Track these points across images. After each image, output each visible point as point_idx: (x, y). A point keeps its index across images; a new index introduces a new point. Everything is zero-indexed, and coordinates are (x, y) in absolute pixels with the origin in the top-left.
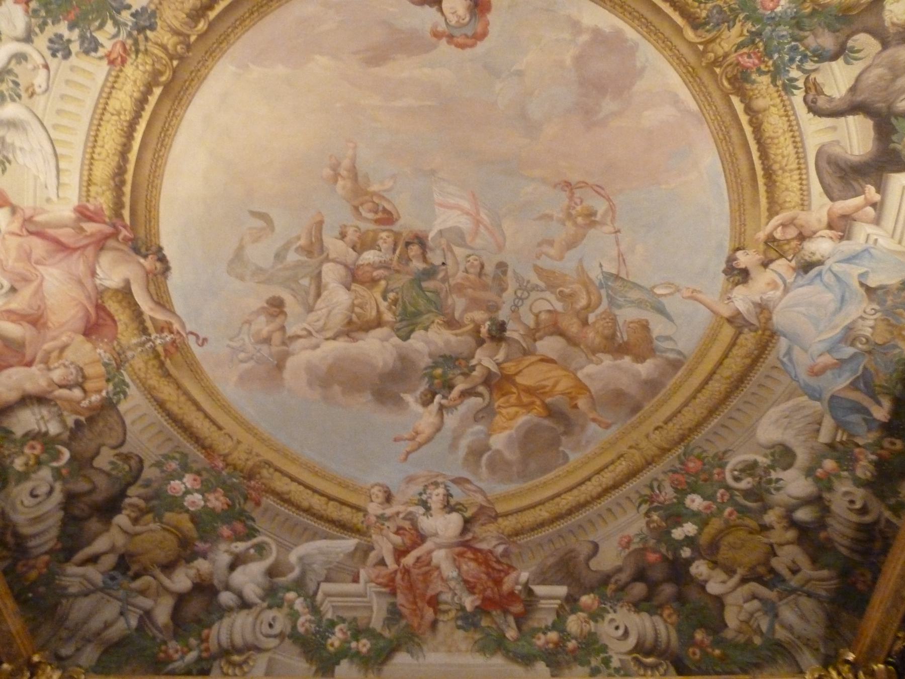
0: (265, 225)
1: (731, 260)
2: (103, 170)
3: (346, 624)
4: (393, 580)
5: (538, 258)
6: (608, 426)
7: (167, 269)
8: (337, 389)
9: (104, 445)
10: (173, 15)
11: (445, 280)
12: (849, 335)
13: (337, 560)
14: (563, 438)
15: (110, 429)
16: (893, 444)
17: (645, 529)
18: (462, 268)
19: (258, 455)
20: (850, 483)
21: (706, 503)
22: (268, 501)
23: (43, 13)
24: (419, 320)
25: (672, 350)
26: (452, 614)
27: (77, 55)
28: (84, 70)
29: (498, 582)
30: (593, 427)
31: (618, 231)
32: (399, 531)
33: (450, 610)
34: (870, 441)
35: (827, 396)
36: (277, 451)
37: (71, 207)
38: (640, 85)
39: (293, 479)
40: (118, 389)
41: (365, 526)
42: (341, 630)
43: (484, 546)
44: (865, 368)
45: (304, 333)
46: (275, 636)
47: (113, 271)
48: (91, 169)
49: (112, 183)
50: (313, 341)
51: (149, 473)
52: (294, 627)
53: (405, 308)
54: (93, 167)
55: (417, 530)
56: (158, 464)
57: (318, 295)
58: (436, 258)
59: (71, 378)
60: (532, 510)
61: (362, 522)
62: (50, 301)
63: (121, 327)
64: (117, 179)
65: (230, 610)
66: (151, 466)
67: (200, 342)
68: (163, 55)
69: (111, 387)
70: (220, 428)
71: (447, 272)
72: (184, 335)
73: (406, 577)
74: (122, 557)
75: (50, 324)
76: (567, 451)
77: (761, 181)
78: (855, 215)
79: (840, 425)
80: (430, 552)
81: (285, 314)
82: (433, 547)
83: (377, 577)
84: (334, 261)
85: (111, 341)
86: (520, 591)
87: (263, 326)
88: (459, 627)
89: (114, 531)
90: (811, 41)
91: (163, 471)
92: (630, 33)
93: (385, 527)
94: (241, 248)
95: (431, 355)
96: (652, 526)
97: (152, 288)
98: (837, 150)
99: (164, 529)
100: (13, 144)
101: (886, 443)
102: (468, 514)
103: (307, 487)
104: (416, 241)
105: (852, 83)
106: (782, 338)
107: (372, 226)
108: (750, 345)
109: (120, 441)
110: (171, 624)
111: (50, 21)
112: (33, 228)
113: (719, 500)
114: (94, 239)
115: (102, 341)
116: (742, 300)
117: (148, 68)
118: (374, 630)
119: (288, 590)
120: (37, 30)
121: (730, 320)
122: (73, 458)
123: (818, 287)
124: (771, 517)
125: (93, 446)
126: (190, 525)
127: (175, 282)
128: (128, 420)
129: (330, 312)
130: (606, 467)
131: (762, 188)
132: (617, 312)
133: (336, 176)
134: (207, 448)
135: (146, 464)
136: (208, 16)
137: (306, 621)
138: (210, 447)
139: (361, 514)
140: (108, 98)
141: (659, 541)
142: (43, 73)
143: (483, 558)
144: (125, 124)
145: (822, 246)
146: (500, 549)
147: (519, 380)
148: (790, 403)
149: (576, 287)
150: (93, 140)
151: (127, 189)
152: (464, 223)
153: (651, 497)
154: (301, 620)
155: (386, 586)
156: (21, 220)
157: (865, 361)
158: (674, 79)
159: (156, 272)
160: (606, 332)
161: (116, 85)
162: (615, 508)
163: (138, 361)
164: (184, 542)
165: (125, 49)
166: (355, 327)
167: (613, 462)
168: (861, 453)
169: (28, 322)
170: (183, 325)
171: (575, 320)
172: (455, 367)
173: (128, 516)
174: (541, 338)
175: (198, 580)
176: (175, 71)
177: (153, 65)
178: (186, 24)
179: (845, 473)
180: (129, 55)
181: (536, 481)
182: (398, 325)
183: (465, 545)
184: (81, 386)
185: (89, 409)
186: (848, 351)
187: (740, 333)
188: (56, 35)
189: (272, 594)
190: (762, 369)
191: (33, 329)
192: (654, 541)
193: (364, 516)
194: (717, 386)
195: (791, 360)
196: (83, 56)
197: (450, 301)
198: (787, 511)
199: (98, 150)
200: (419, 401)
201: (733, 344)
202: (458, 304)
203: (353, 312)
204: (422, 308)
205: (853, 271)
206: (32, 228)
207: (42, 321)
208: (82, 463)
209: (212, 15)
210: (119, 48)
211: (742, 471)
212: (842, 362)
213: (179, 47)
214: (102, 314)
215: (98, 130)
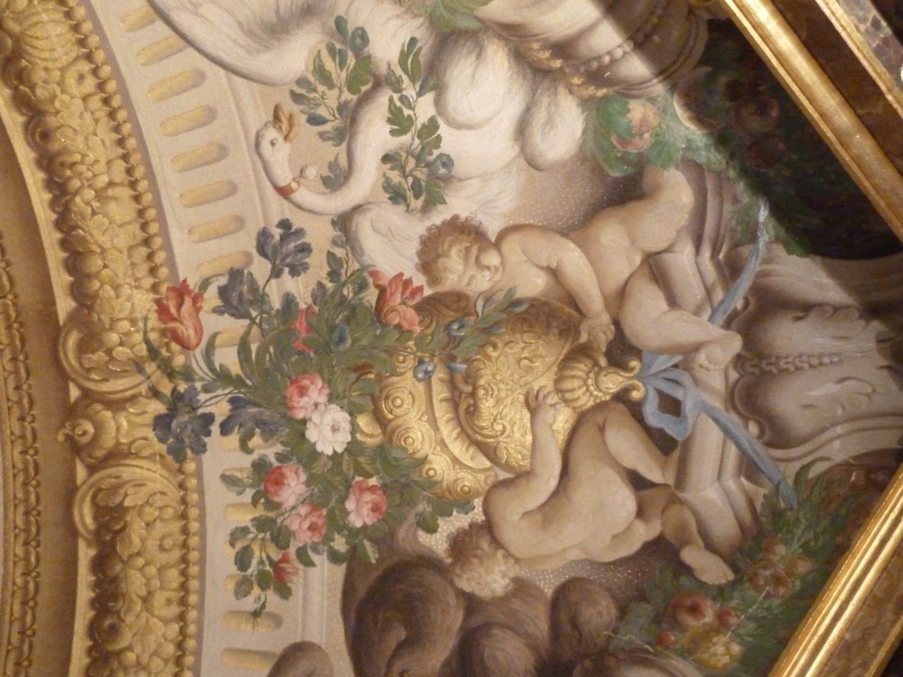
10: (147, 479)
23: (348, 291)
27: (249, 260)
28: (219, 236)
48: (76, 28)
49: (14, 27)
54: (72, 37)
64: (9, 43)
68: (105, 387)
111: (329, 285)
120: (340, 252)
136: (89, 544)
140: (141, 213)
142: (284, 177)
144: (75, 183)
150: (112, 102)
161: (144, 251)
176: (64, 377)
177: (109, 352)
178: (115, 489)
180: (163, 332)
188: (305, 267)
196: (237, 266)
199: (90, 83)
209: (86, 554)
210: (187, 330)
213: (89, 427)
215: (117, 129)
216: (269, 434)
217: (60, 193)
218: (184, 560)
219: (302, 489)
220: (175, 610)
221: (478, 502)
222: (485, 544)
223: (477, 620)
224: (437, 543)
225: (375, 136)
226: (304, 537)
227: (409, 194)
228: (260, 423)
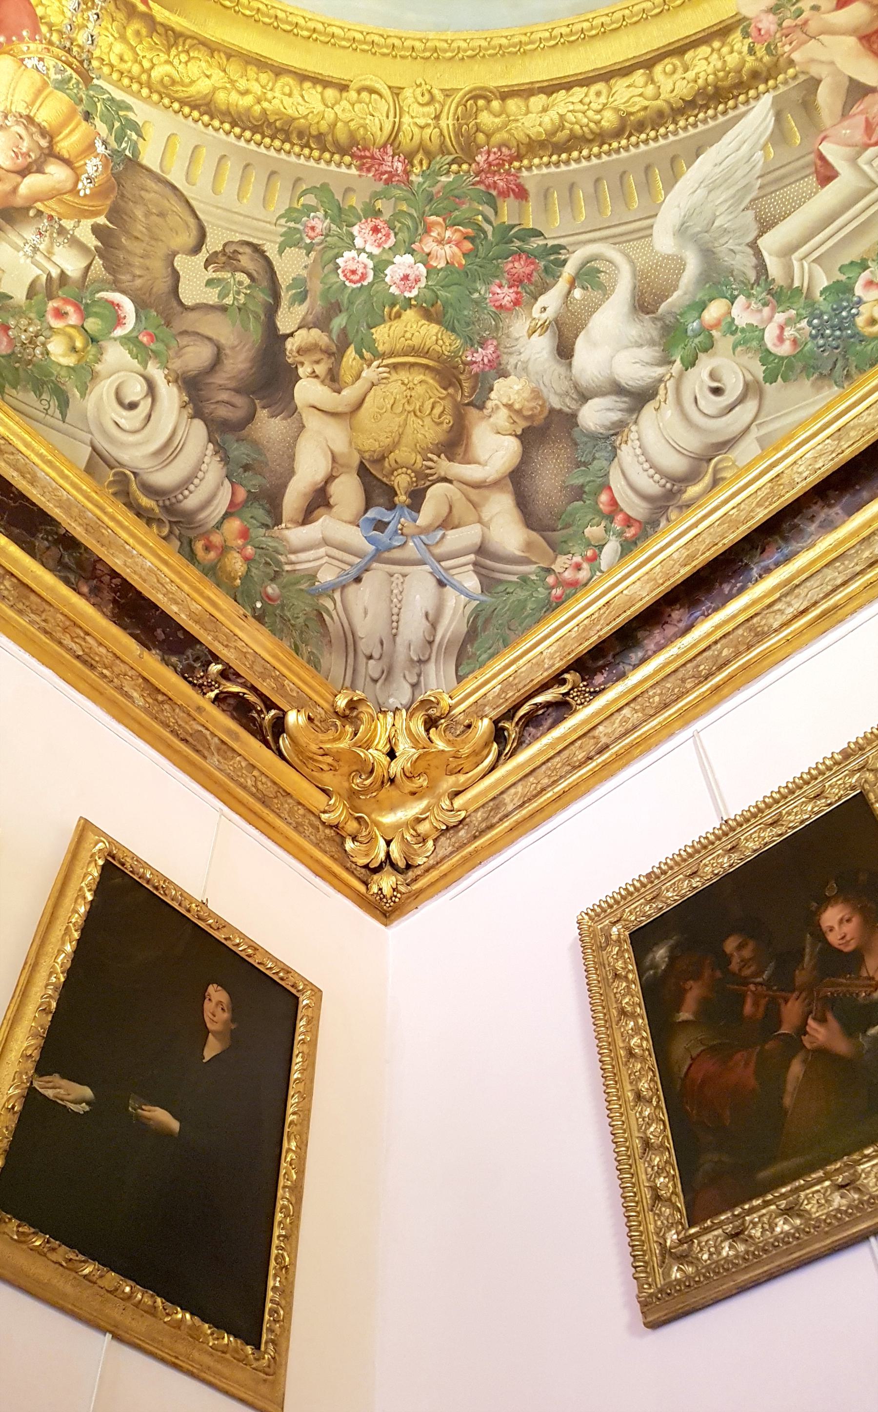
9: (174, 254)
13: (757, 171)
15: (162, 215)
19: (448, 93)
22: (535, 173)
36: (477, 55)
39: (550, 89)
40: (117, 124)
41: (761, 51)
46: (741, 400)
51: (290, 266)
52: (766, 356)
56: (290, 240)
59: (25, 146)
61: (751, 51)
65: (618, 428)
66: (281, 252)
69: (102, 128)
70: (343, 88)
74: (363, 471)
85: (36, 30)
89: (313, 422)
91: (309, 249)
99: (395, 367)
103: (586, 81)
109: (194, 232)
110: (534, 535)
119: (702, 306)
122: (141, 305)
125: (158, 265)
126: (434, 328)
128: (176, 177)
134: (353, 148)
135: (271, 251)
137: (782, 328)
138: (353, 141)
139: (737, 36)
154: (770, 335)
164: (448, 373)
173: (314, 375)
175: (524, 424)
184: (51, 154)
185: (100, 193)
189: (676, 338)
193: (746, 34)
208: (164, 306)
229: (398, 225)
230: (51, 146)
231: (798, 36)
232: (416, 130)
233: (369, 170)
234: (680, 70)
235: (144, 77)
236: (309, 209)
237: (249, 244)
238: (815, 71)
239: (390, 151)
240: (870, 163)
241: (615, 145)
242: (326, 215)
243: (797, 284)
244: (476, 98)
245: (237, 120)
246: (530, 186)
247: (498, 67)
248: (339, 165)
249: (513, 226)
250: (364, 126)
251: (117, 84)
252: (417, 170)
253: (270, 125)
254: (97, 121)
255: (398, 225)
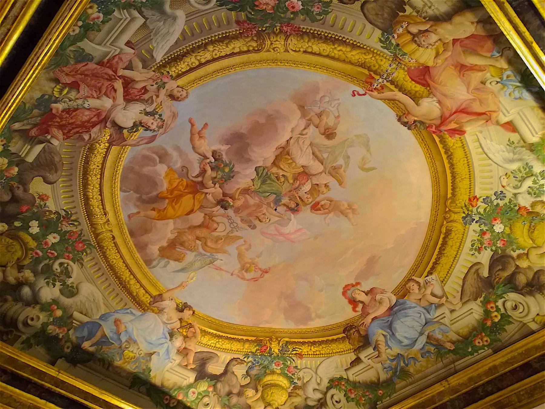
0: (365, 167)
1: (190, 308)
2: (458, 154)
3: (99, 23)
4: (110, 67)
5: (245, 241)
6: (129, 216)
7: (399, 120)
8: (262, 121)
10: (458, 227)
11: (268, 204)
12: (131, 341)
13: (153, 41)
14: (138, 195)
16: (68, 348)
17: (47, 209)
18: (267, 214)
19: (268, 51)
20: (45, 321)
21: (50, 244)
22: (234, 29)
23: (512, 206)
24: (260, 181)
25: (158, 265)
26: (56, 94)
27: (492, 195)
29: (61, 127)
30: (135, 210)
31: (232, 275)
32: (145, 90)
33: (61, 94)
34: (71, 337)
35: (101, 323)
37: (467, 132)
38: (282, 316)
39: (233, 54)
40: (388, 42)
41: (165, 72)
42: (98, 18)
43: (96, 129)
44: (113, 344)
45: (304, 132)
47: (429, 108)
49: (452, 151)
50: (297, 132)
53: (271, 179)
55: (137, 100)
57: (313, 154)
58: (281, 209)
59: (424, 38)
60: (101, 162)
61: (168, 72)
62: (458, 80)
63: (408, 78)
67: (356, 93)
69: (393, 41)
70: (305, 52)
71: (271, 207)
72: (367, 91)
73: (106, 76)
75: (453, 68)
76: (127, 193)
77: (218, 333)
78: (186, 358)
79: (83, 325)
80: (114, 99)
81: (323, 134)
82: (117, 102)
83: (121, 59)
84: (321, 173)
85: (408, 69)
86: (46, 137)
87: (330, 121)
88: (43, 96)
90: (257, 368)
92: (302, 327)
93: (154, 84)
94: (368, 150)
95: (238, 172)
96: (47, 213)
97: (402, 106)
98: (215, 360)
100: (509, 153)
101: (69, 344)
102: (125, 131)
104: (296, 208)
105: (235, 373)
106: (141, 313)
107: (318, 199)
108: (144, 298)
111: (508, 204)
112: (485, 116)
113: (49, 251)
114: (448, 120)
115: (415, 67)
116: (169, 305)
117: (457, 202)
118: (81, 40)
120: (512, 199)
121: (160, 295)
123: (161, 335)
124: (28, 274)
127: (391, 115)
128: (369, 26)
129: (302, 151)
130: (103, 205)
131: (215, 332)
132: (194, 254)
133: (350, 207)
134: (301, 34)
139: (174, 75)
141: (34, 213)
142: (504, 184)
143: (87, 126)
144: (457, 177)
145: (178, 342)
146: (86, 137)
147: (190, 196)
148: (102, 305)
149: (219, 246)
151: (442, 151)
152: (286, 230)
153: (69, 218)
155: (109, 61)
156: (492, 119)
157: (116, 344)
158: (275, 326)
159: (405, 116)
160: (187, 244)
162: (71, 200)
163: (385, 65)
165: (471, 204)
166: (284, 153)
167: (104, 209)
168: (64, 330)
169: (466, 66)
170: (370, 95)
171: (203, 236)
172: (222, 177)
174: (204, 217)
176: (446, 207)
179: (52, 320)
181: (120, 172)
182: (266, 170)
183: (103, 119)
184: (414, 35)
185: (399, 22)
186: (124, 338)
187: (151, 297)
190: (127, 299)
191: (462, 63)
192: (36, 211)
193: (171, 76)
194: (126, 275)
195: (128, 313)
197: (257, 198)
198: (31, 283)
199: (466, 162)
200: (219, 151)
201: (147, 292)
202: (252, 201)
203: (291, 159)
204: (264, 186)
205: (162, 351)
206: (485, 116)
207: (459, 68)
209: (442, 236)
210: (474, 204)
211: (66, 268)
212: (118, 334)
214: (425, 82)
216: (485, 225)
217: (454, 177)
218: (461, 242)
219: (489, 237)
220: (457, 249)
221: (527, 249)
222: (525, 257)
223: (517, 271)
224: (515, 254)
225: (529, 182)
226: (487, 245)
227: (533, 194)
228: (484, 223)
229: (284, 9)
230: (413, 38)
231: (155, 78)
232: (279, 40)
233: (296, 27)
234: (190, 64)
235: (375, 55)
236: (320, 14)
237: (345, 4)
238: (145, 71)
239: (288, 34)
240: (116, 50)
241: (207, 41)
242: (313, 12)
243: (125, 11)
244: (258, 50)
245: (344, 42)
246: (235, 25)
247: (251, 59)
248: (307, 28)
249: (239, 11)
250: (297, 40)
251: (385, 53)
252: (278, 28)
253: (332, 41)
254: (395, 44)
255: (284, 9)
